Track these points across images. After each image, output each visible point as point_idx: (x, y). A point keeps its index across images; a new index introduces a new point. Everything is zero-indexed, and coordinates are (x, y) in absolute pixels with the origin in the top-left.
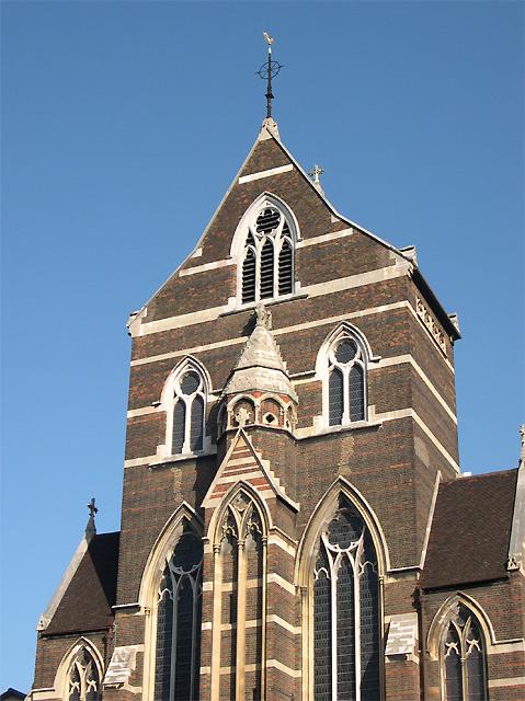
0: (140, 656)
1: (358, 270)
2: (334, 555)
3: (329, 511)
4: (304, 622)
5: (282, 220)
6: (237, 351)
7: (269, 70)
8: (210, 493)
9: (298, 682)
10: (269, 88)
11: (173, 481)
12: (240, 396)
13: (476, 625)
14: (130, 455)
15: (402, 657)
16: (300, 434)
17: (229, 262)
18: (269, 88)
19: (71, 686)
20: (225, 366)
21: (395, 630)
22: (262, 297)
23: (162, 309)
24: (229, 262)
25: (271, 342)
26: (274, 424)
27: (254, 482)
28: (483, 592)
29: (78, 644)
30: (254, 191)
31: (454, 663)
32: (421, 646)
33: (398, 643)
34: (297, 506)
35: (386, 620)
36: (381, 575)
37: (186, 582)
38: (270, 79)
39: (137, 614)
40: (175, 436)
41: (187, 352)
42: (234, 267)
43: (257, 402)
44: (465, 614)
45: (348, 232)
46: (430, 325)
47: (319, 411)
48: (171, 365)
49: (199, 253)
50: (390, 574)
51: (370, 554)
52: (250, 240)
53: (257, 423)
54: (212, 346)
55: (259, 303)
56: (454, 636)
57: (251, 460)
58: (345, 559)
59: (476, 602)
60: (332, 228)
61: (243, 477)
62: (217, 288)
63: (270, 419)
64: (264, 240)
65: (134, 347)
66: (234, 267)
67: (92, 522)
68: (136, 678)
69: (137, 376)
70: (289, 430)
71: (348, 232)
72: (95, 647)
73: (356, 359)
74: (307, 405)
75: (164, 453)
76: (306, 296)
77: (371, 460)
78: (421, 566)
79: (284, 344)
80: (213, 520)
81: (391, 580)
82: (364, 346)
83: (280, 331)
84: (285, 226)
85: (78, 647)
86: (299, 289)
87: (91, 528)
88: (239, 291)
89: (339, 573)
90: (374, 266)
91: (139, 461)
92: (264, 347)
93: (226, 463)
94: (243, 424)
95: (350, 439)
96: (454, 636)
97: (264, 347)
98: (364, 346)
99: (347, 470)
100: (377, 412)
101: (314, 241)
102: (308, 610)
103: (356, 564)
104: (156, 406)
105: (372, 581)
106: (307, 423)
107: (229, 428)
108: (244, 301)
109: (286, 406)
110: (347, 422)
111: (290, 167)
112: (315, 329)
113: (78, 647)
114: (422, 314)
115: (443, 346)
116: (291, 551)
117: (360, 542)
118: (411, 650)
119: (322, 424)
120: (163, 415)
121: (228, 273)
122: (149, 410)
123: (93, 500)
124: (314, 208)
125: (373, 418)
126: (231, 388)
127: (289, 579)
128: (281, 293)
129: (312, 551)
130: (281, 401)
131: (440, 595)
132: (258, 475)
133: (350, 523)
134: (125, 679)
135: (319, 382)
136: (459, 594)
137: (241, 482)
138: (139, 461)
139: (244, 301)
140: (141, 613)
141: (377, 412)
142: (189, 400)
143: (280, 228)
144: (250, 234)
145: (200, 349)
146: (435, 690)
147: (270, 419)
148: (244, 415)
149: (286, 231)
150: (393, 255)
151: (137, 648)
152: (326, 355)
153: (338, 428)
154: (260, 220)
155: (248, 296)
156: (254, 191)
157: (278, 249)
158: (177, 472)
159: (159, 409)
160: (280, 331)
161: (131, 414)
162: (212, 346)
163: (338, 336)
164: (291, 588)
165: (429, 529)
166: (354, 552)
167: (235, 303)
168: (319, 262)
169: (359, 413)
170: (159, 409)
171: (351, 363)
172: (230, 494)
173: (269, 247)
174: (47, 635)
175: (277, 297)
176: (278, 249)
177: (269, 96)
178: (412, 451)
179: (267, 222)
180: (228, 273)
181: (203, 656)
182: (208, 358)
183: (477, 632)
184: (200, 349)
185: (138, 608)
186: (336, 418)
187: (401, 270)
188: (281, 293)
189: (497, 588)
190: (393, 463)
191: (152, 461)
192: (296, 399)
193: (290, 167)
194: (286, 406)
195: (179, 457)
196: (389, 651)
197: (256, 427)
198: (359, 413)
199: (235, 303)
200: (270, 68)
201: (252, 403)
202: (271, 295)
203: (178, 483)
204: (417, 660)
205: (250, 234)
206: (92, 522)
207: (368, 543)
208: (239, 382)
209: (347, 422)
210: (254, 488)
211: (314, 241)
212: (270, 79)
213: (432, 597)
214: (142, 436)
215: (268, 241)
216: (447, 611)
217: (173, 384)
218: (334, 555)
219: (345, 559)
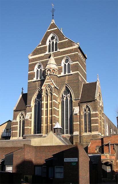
0: (31, 114)
1: (69, 46)
2: (65, 97)
3: (64, 89)
4: (59, 108)
5: (55, 38)
6: (47, 61)
7: (53, 11)
8: (43, 86)
9: (58, 118)
10: (53, 14)
11: (36, 84)
12: (48, 69)
13: (89, 109)
14: (29, 80)
15: (76, 114)
16: (59, 76)
17: (46, 45)
18: (53, 14)
20: (45, 64)
21: (75, 110)
22: (52, 51)
23: (34, 54)
24: (46, 45)
25: (54, 60)
26: (54, 74)
27: (50, 84)
28: (90, 103)
30: (50, 32)
31: (85, 115)
32: (80, 112)
33: (76, 112)
34: (58, 88)
35: (73, 108)
36: (73, 100)
37: (39, 101)
38: (53, 12)
40: (37, 76)
41: (39, 61)
42: (47, 46)
43: (51, 70)
44: (87, 107)
45: (67, 40)
46: (82, 56)
47: (62, 72)
48: (36, 64)
49: (41, 44)
50: (74, 100)
51: (71, 96)
52: (50, 41)
53: (51, 74)
54: (43, 60)
55: (51, 53)
56: (85, 111)
57: (50, 80)
58: (67, 97)
59: (89, 105)
60: (64, 39)
61: (49, 83)
62: (43, 50)
63: (53, 73)
64: (52, 41)
65: (29, 61)
66: (47, 46)
67: (22, 91)
68: (31, 118)
69: (30, 65)
70: (57, 75)
71: (67, 40)
72: (23, 113)
73: (69, 62)
74: (60, 71)
75: (35, 79)
77: (71, 80)
78: (80, 99)
79: (56, 60)
80: (44, 91)
81: (75, 101)
82: (70, 60)
83: (55, 58)
85: (21, 113)
86: (58, 50)
87: (22, 92)
88: (48, 51)
89: (66, 100)
90: (72, 46)
91: (30, 81)
92: (52, 60)
93: (46, 81)
94: (49, 74)
95: (67, 77)
96: (85, 111)
97: (52, 60)
98: (70, 60)
99: (67, 82)
100: (72, 72)
101: (61, 41)
102: (60, 106)
103: (69, 98)
105: (71, 101)
106: (60, 74)
107: (46, 75)
108: (49, 52)
109: (56, 71)
110: (67, 74)
111: (57, 28)
113: (21, 113)
114: (80, 55)
115: (84, 60)
116: (57, 96)
117: (69, 94)
118: (78, 113)
119: (62, 74)
120: (35, 73)
121: (46, 47)
122: (32, 72)
124: (61, 36)
125: (71, 73)
126: (46, 68)
127: (57, 101)
128: (55, 51)
129: (61, 96)
130: (55, 70)
131: (84, 103)
132: (51, 83)
133: (67, 91)
134: (29, 118)
135: (62, 66)
138: (30, 81)
139: (49, 52)
141: (72, 72)
142: (39, 70)
143: (55, 39)
144: (50, 40)
145: (41, 61)
146: (82, 120)
147: (53, 73)
148: (49, 72)
149: (56, 40)
150: (75, 44)
151: (31, 113)
152: (63, 61)
153: (65, 74)
154: (51, 38)
155: (49, 51)
156: (50, 32)
157: (55, 43)
158: (37, 82)
159: (34, 71)
160: (55, 58)
161: (29, 72)
162: (43, 60)
163: (65, 58)
164: (57, 102)
165: (81, 92)
166: (68, 96)
167: (47, 53)
168: (62, 45)
169: (69, 72)
170: (34, 71)
171: (68, 63)
172: (46, 86)
173: (53, 42)
174: (15, 111)
175: (55, 52)
176: (55, 43)
177: (53, 15)
178: (78, 79)
179: (53, 38)
180: (46, 47)
181: (42, 106)
182: (42, 63)
183: (89, 110)
184: (41, 61)
185: (31, 106)
186: (65, 73)
187: (76, 46)
188: (55, 51)
189: (93, 102)
190: (75, 81)
191: (33, 80)
192: (58, 69)
193: (57, 28)
194: (56, 71)
195: (37, 80)
196: (74, 113)
197: (51, 74)
198: (69, 72)
199: (47, 53)
200: (53, 10)
201: (50, 70)
202: (54, 51)
203: (37, 84)
204: (79, 115)
205: (50, 40)
206: (22, 91)
207: (71, 95)
208: (48, 67)
209: (67, 74)
211: (61, 41)
212: (53, 12)
213: (81, 104)
214: (31, 76)
215: (53, 41)
216: (84, 106)
217: (36, 67)
218: (65, 97)
219: (67, 97)
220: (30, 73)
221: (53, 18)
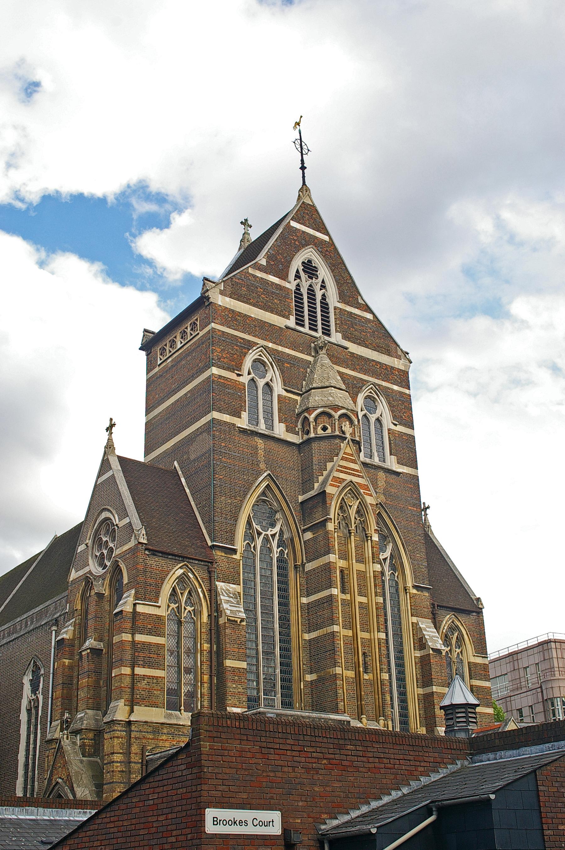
12: (343, 411)
19: (169, 606)
29: (181, 568)
39: (234, 556)
50: (415, 587)
54: (280, 348)
61: (355, 479)
64: (309, 283)
71: (369, 316)
76: (347, 348)
80: (333, 503)
81: (414, 591)
84: (323, 282)
85: (181, 571)
87: (110, 447)
104: (239, 375)
112: (355, 378)
123: (111, 419)
136: (454, 615)
137: (351, 481)
140: (237, 556)
147: (324, 429)
183: (460, 641)
185: (234, 551)
201: (330, 416)
206: (110, 440)
210: (362, 491)
220: (220, 376)
221: (304, 177)
